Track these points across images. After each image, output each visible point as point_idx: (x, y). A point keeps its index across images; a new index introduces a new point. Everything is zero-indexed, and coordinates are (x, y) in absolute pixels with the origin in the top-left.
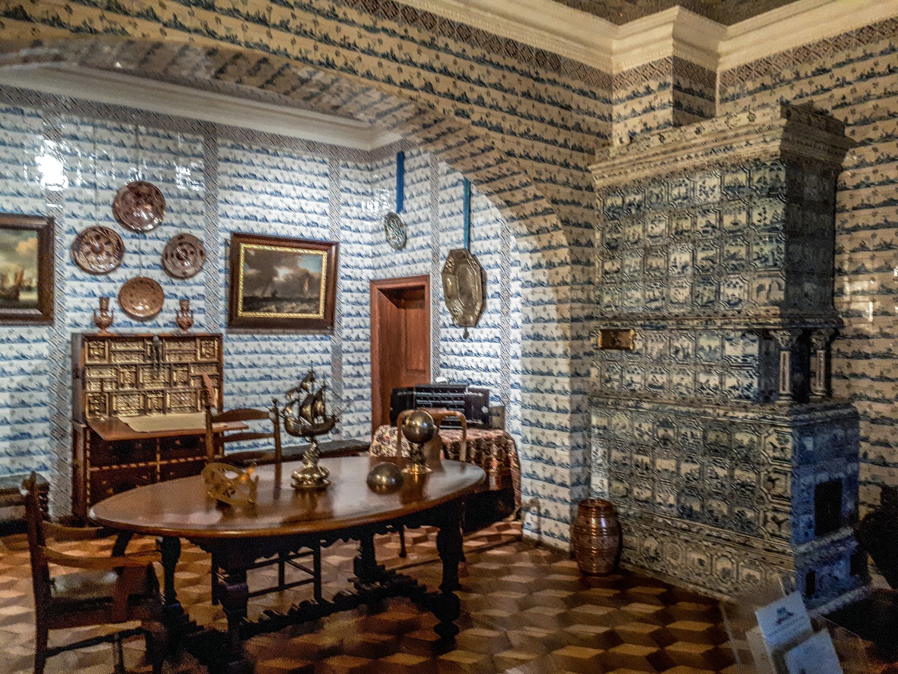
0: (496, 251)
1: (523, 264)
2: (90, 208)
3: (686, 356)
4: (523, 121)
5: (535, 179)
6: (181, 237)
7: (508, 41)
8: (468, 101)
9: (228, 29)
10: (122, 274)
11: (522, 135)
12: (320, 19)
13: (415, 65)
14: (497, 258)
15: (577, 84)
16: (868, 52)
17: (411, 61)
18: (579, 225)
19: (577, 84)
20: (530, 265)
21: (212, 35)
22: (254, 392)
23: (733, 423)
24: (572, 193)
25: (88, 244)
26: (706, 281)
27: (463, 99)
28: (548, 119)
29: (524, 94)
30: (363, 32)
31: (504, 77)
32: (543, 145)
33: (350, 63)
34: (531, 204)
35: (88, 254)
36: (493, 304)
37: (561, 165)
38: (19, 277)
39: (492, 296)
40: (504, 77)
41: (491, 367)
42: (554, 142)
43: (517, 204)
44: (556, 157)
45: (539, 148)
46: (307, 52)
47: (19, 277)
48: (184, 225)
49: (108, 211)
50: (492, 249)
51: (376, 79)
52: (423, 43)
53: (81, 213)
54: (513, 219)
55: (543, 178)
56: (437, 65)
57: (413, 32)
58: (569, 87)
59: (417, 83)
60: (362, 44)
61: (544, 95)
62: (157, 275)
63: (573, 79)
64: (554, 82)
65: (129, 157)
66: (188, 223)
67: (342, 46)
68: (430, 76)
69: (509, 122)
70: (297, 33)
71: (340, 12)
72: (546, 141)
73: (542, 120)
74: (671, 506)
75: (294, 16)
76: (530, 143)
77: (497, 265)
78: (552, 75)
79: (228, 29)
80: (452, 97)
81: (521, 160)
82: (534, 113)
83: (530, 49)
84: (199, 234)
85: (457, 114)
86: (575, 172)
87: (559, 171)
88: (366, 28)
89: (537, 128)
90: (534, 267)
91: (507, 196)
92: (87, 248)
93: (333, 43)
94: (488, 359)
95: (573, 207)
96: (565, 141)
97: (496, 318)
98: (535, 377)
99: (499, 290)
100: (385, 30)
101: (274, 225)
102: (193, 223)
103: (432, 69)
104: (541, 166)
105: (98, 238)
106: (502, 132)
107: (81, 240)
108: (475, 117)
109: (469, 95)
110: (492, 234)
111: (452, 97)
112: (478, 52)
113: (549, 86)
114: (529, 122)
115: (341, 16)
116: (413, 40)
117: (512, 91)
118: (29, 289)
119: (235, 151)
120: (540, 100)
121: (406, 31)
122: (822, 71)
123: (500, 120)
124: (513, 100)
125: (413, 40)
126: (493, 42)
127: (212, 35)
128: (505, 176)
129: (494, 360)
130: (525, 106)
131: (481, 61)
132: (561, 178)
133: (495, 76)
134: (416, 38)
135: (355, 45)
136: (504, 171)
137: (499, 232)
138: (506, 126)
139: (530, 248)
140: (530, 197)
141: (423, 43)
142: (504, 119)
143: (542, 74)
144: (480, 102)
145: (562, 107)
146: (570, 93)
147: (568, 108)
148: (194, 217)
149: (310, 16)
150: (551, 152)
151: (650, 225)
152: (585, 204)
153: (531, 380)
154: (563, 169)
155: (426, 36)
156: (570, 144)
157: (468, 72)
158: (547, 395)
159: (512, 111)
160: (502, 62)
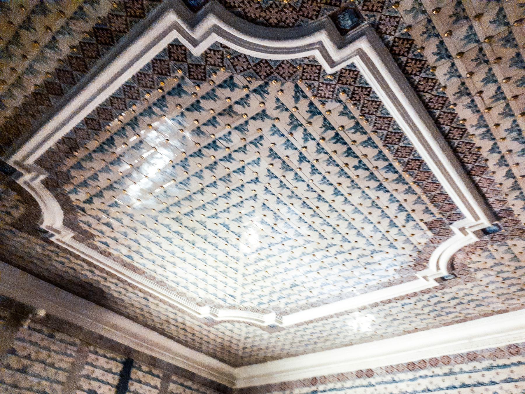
7: (510, 347)
12: (388, 386)
13: (442, 389)
40: (512, 372)
52: (445, 374)
56: (457, 384)
57: (437, 370)
71: (396, 379)
88: (410, 380)
100: (421, 377)
112: (486, 363)
116: (439, 375)
121: (433, 372)
125: (439, 375)
126: (496, 353)
131: (490, 368)
133: (504, 374)
134: (441, 373)
141: (445, 374)
149: (383, 386)
155: (446, 369)
157: (482, 380)
160: (508, 362)
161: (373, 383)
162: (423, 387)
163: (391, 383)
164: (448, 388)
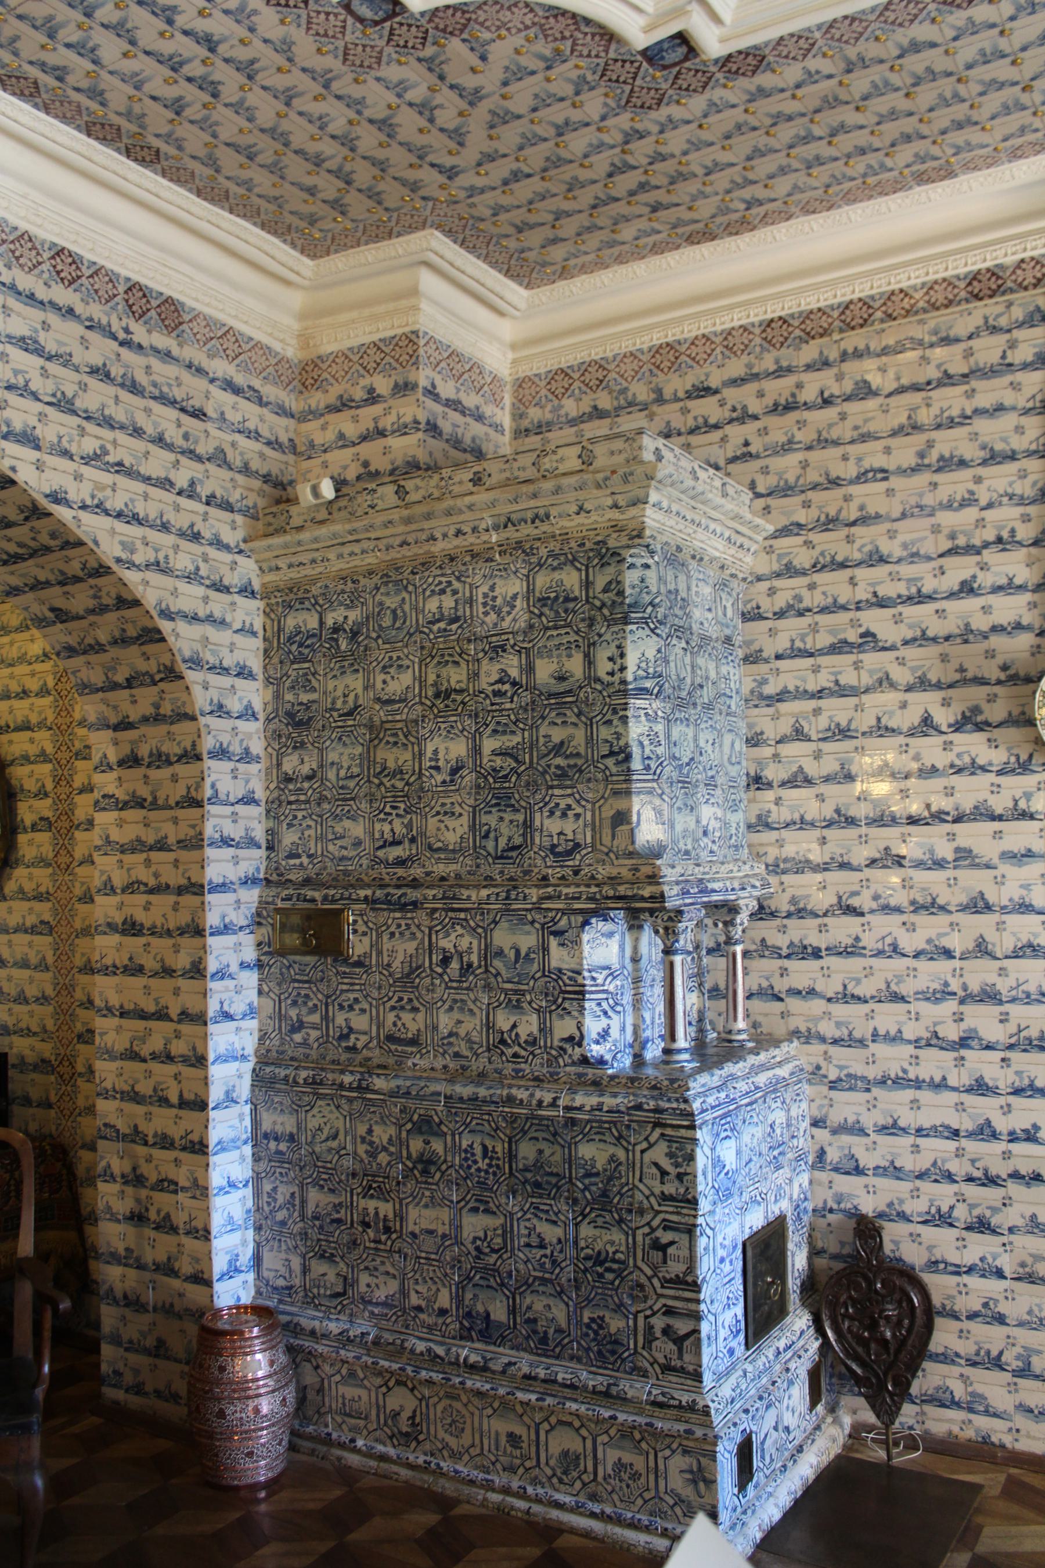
0: (42, 725)
1: (96, 758)
3: (467, 969)
4: (90, 427)
11: (88, 460)
14: (44, 740)
15: (220, 367)
16: (785, 364)
18: (225, 671)
19: (220, 367)
20: (113, 758)
23: (573, 1122)
24: (206, 599)
26: (503, 801)
28: (150, 430)
29: (94, 371)
31: (46, 326)
32: (139, 487)
34: (112, 617)
36: (32, 845)
37: (182, 534)
39: (34, 828)
40: (46, 326)
41: (31, 992)
42: (166, 484)
43: (78, 618)
44: (170, 516)
50: (34, 719)
54: (71, 651)
55: (138, 559)
58: (200, 371)
61: (142, 378)
63: (211, 356)
64: (167, 356)
69: (57, 427)
72: (147, 479)
73: (137, 432)
74: (443, 1312)
76: (107, 478)
77: (43, 757)
78: (161, 340)
82: (119, 415)
83: (112, 278)
86: (213, 553)
89: (126, 448)
90: (121, 763)
91: (55, 595)
94: (27, 973)
96: (192, 483)
97: (42, 878)
98: (126, 1023)
99: (48, 814)
104: (135, 531)
106: (38, 448)
110: (33, 685)
113: (155, 363)
114: (107, 434)
117: (65, 360)
120: (134, 388)
122: (703, 391)
123: (33, 421)
124: (68, 381)
128: (47, 549)
129: (38, 975)
130: (97, 396)
132: (183, 562)
136: (45, 539)
137: (51, 683)
138: (48, 434)
139: (113, 720)
140: (106, 601)
142: (42, 416)
143: (140, 333)
145: (183, 410)
146: (202, 383)
147: (199, 414)
150: (157, 504)
151: (380, 677)
152: (237, 626)
153: (119, 1029)
154: (185, 545)
156: (204, 491)
158: (155, 1067)
159: (64, 404)
160: (42, 293)
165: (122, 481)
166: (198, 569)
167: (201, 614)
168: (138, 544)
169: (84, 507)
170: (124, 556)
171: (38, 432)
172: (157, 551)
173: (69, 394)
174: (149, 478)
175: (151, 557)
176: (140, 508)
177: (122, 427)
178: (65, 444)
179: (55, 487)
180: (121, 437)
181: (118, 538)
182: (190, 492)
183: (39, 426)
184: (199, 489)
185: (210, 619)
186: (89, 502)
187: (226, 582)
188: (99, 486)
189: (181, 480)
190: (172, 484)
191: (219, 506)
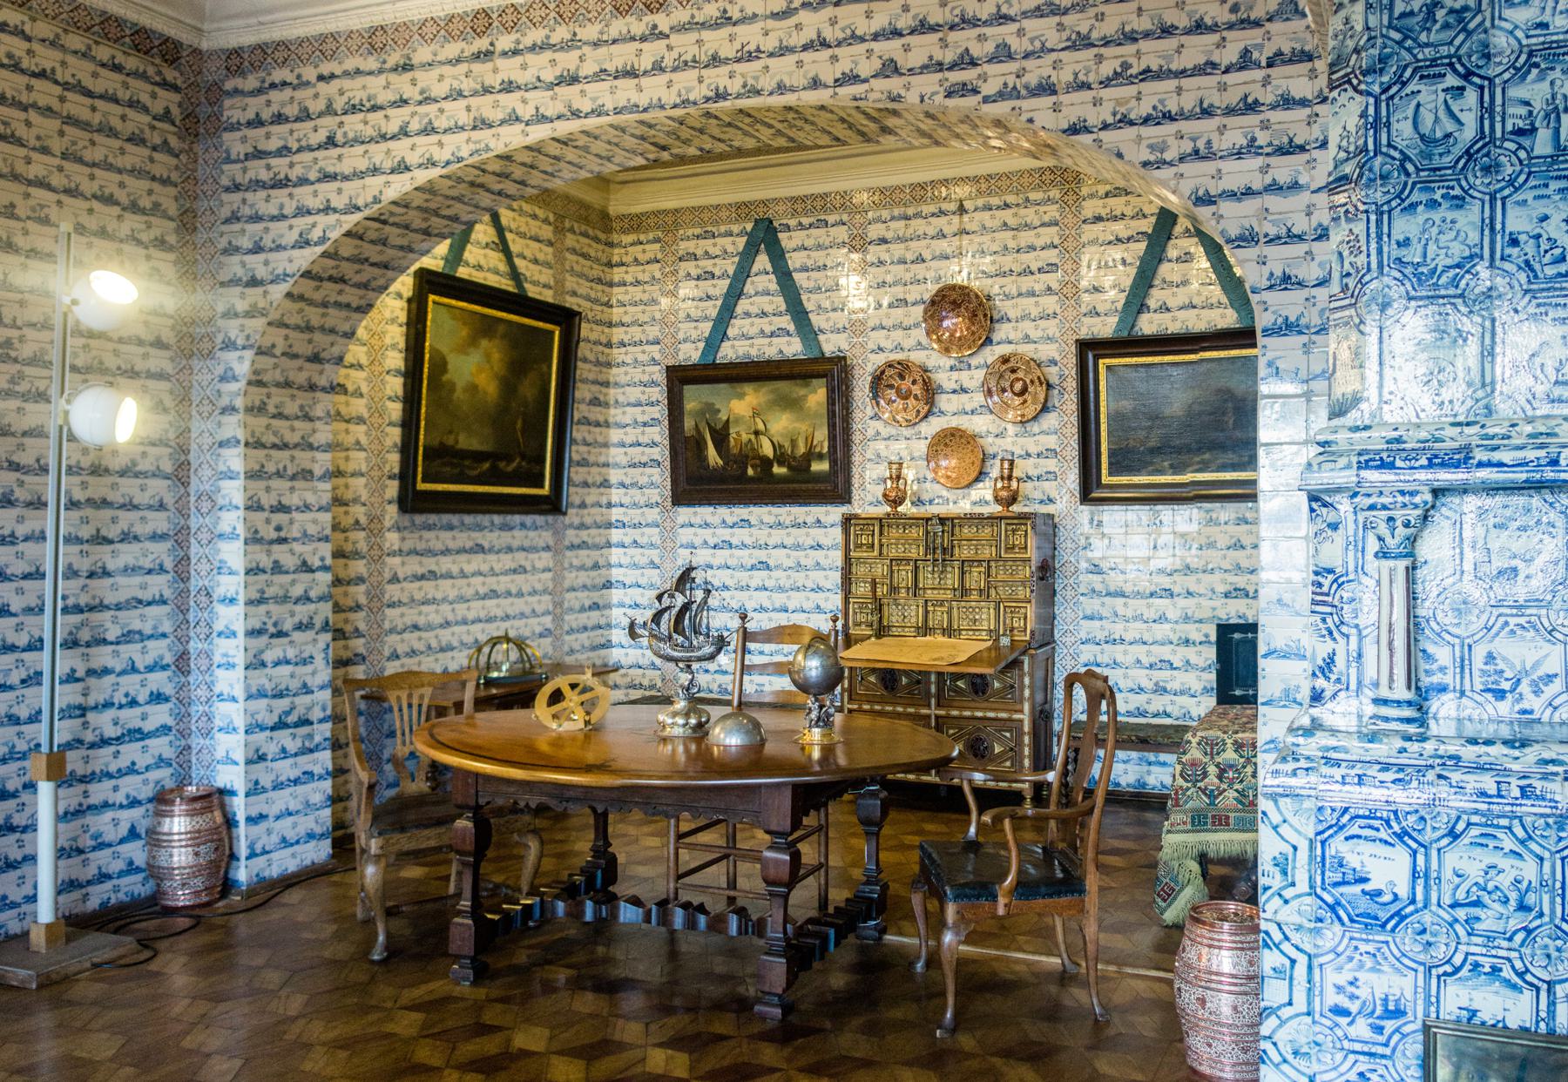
2: (898, 335)
5: (1145, 164)
6: (1005, 360)
8: (973, 63)
9: (594, 100)
10: (934, 426)
11: (1106, 83)
13: (862, 40)
17: (853, 36)
21: (576, 114)
22: (1138, 618)
24: (1264, 170)
25: (891, 387)
27: (967, 61)
30: (771, 23)
32: (1171, 84)
33: (750, 82)
35: (890, 402)
37: (1230, 111)
38: (809, 440)
42: (1208, 68)
45: (1155, 94)
46: (689, 90)
47: (809, 440)
48: (1027, 339)
49: (920, 334)
51: (792, 90)
53: (888, 345)
55: (1168, 156)
59: (865, 69)
60: (770, 44)
62: (978, 424)
65: (949, 251)
66: (1034, 335)
67: (738, 60)
68: (891, 48)
69: (1076, 63)
70: (675, 70)
72: (1182, 73)
75: (670, 48)
79: (594, 100)
80: (940, 67)
81: (1103, 135)
84: (1046, 351)
85: (949, 95)
87: (1222, 129)
89: (1152, 53)
92: (892, 394)
93: (726, 61)
95: (1272, 201)
96: (1246, 53)
101: (1182, 314)
102: (1039, 333)
103: (897, 33)
104: (1169, 129)
105: (902, 377)
106: (1054, 92)
107: (878, 382)
108: (989, 89)
109: (976, 50)
111: (940, 67)
114: (1129, 49)
115: (736, 16)
118: (820, 457)
119: (1111, 201)
127: (576, 114)
135: (758, 50)
144: (1003, 53)
148: (1043, 323)
149: (692, 36)
159: (1081, 42)
161: (664, 26)
162: (809, 34)
163: (716, 25)
164: (876, 37)
165: (1148, 87)
166: (1254, 139)
167: (1257, 185)
168: (1171, 141)
169: (1105, 127)
170: (1152, 158)
171: (1054, 79)
172: (1194, 140)
173: (1084, 31)
174: (1184, 71)
175: (1187, 147)
176: (1172, 107)
177: (1147, 35)
178: (1081, 77)
179: (1073, 119)
180: (1144, 45)
181: (1145, 143)
182: (1246, 61)
183: (1054, 74)
184: (1255, 55)
185: (1274, 188)
186: (1110, 120)
187: (1298, 141)
188: (1118, 102)
189: (1230, 55)
190: (1214, 65)
191: (1291, 61)
